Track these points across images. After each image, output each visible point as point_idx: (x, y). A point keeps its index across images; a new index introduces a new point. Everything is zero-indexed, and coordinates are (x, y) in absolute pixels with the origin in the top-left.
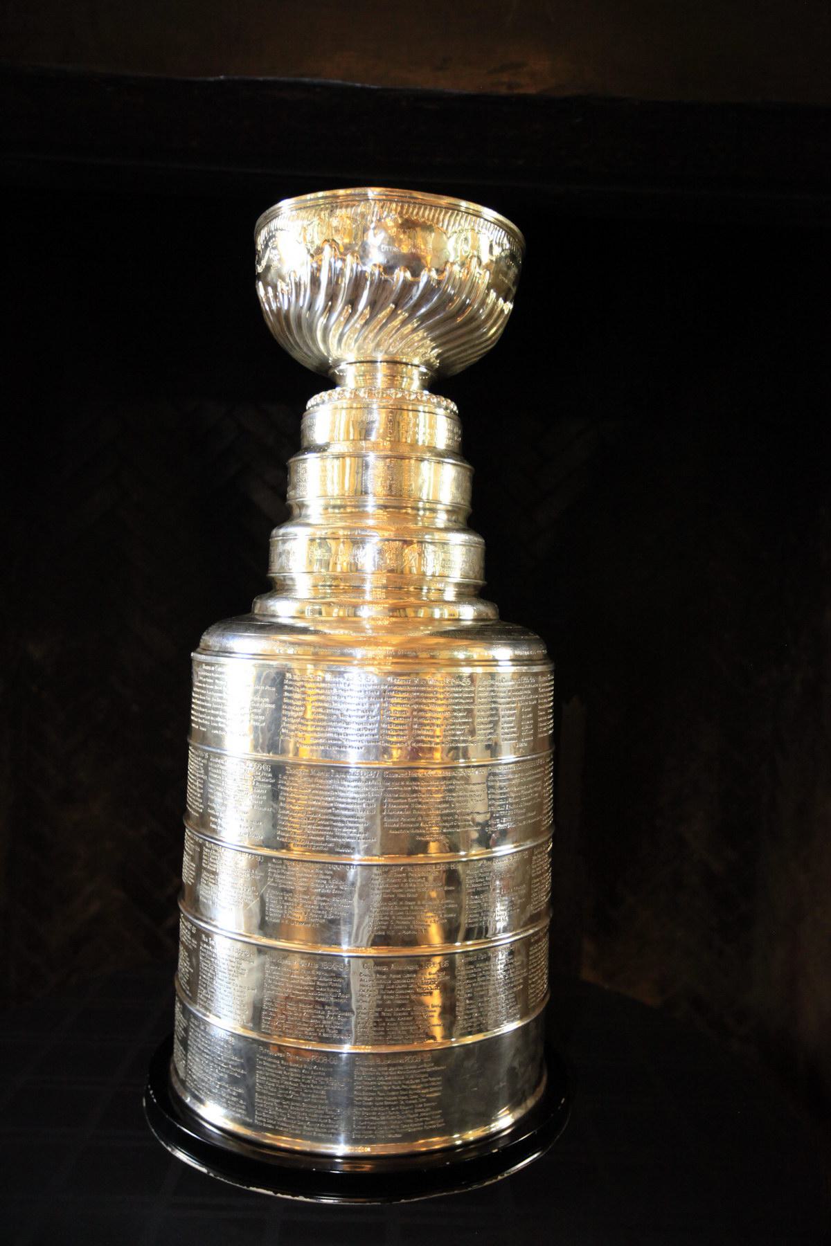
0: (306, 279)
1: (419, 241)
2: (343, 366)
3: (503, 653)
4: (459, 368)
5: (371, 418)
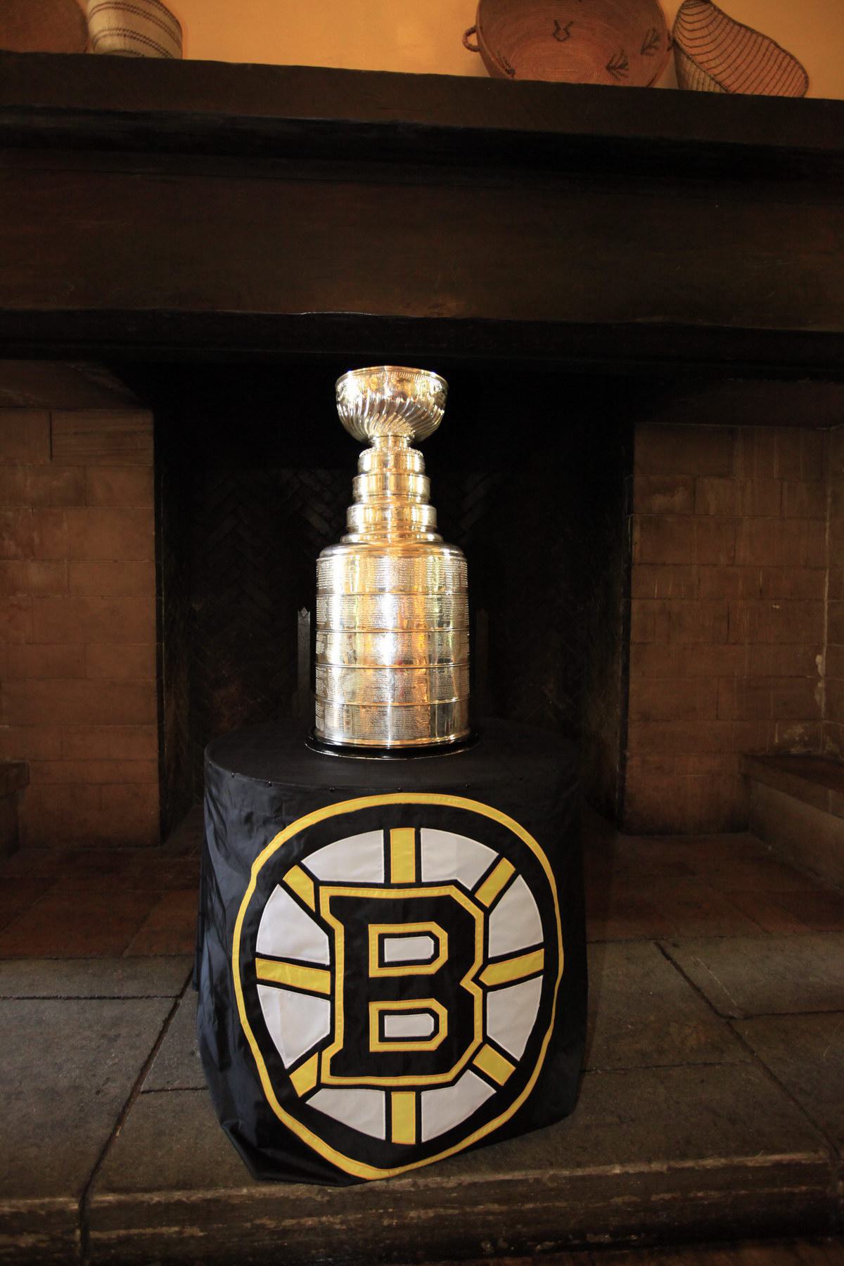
0: (360, 404)
1: (406, 387)
2: (374, 438)
3: (446, 551)
4: (423, 438)
5: (389, 458)
